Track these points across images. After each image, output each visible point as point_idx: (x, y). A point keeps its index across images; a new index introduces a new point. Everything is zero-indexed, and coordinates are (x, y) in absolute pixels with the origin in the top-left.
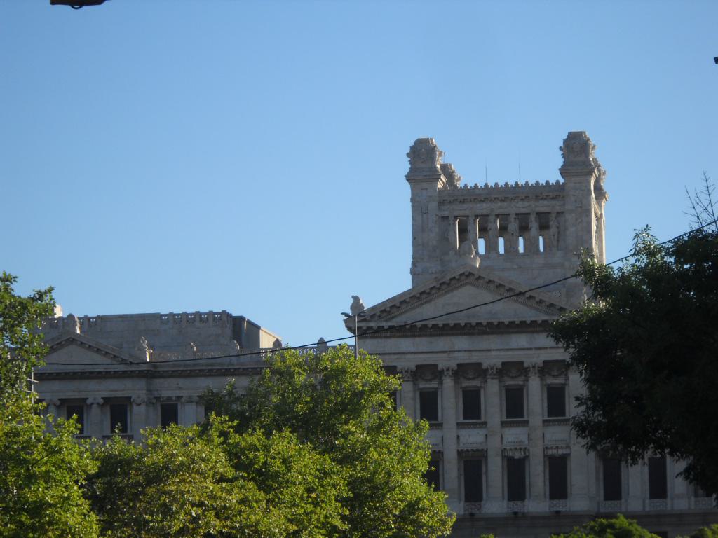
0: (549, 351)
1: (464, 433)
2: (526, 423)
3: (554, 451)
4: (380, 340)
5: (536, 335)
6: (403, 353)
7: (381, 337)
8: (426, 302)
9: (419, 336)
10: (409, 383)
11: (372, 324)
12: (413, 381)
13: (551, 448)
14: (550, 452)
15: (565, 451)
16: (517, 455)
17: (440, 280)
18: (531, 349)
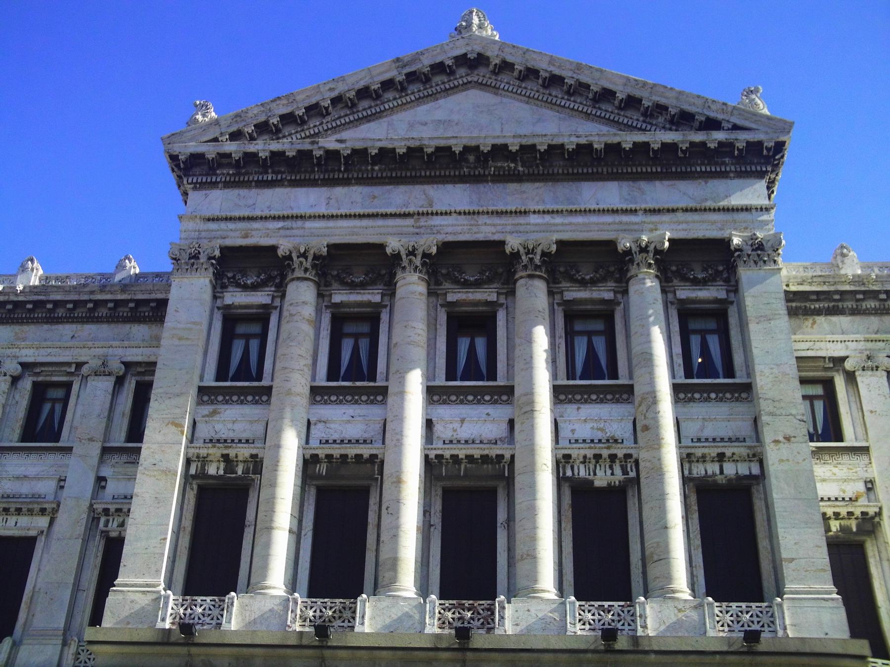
0: (680, 216)
1: (445, 413)
2: (625, 393)
3: (713, 468)
4: (243, 192)
5: (643, 184)
6: (302, 217)
7: (247, 184)
8: (368, 119)
9: (345, 182)
10: (306, 283)
11: (231, 147)
12: (318, 285)
13: (703, 459)
14: (699, 470)
15: (743, 469)
16: (602, 478)
17: (404, 66)
18: (634, 212)
